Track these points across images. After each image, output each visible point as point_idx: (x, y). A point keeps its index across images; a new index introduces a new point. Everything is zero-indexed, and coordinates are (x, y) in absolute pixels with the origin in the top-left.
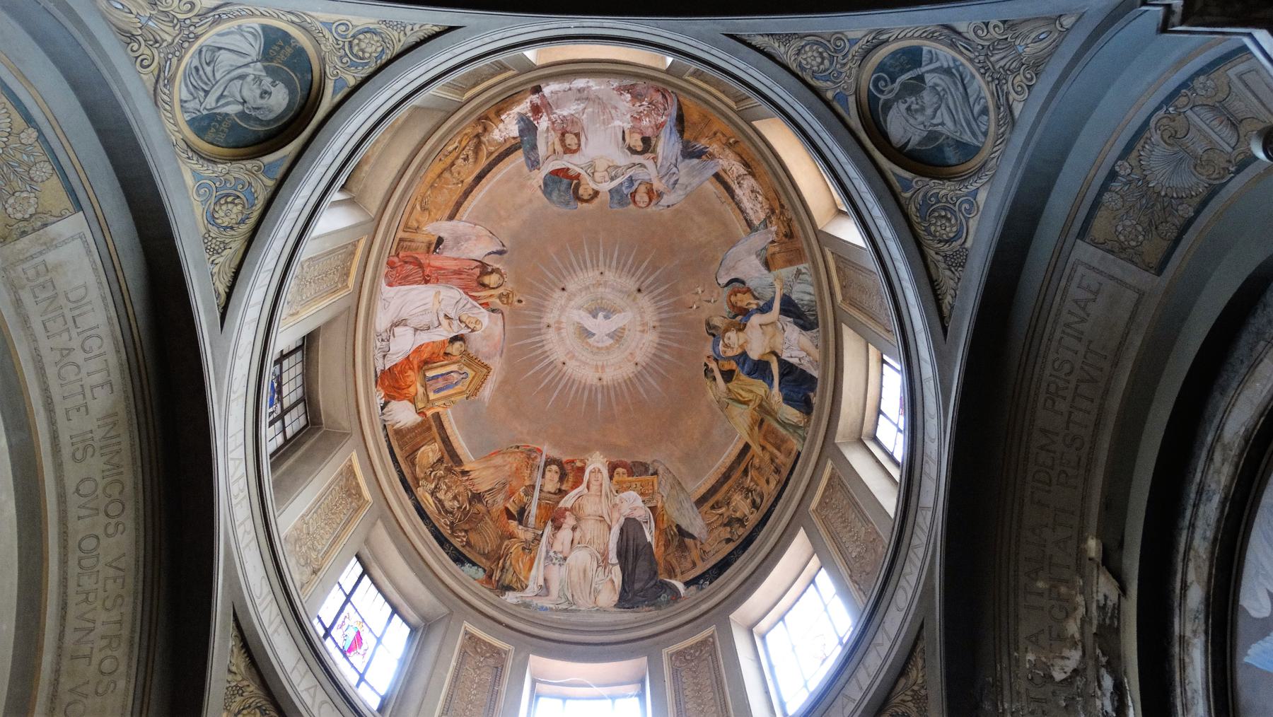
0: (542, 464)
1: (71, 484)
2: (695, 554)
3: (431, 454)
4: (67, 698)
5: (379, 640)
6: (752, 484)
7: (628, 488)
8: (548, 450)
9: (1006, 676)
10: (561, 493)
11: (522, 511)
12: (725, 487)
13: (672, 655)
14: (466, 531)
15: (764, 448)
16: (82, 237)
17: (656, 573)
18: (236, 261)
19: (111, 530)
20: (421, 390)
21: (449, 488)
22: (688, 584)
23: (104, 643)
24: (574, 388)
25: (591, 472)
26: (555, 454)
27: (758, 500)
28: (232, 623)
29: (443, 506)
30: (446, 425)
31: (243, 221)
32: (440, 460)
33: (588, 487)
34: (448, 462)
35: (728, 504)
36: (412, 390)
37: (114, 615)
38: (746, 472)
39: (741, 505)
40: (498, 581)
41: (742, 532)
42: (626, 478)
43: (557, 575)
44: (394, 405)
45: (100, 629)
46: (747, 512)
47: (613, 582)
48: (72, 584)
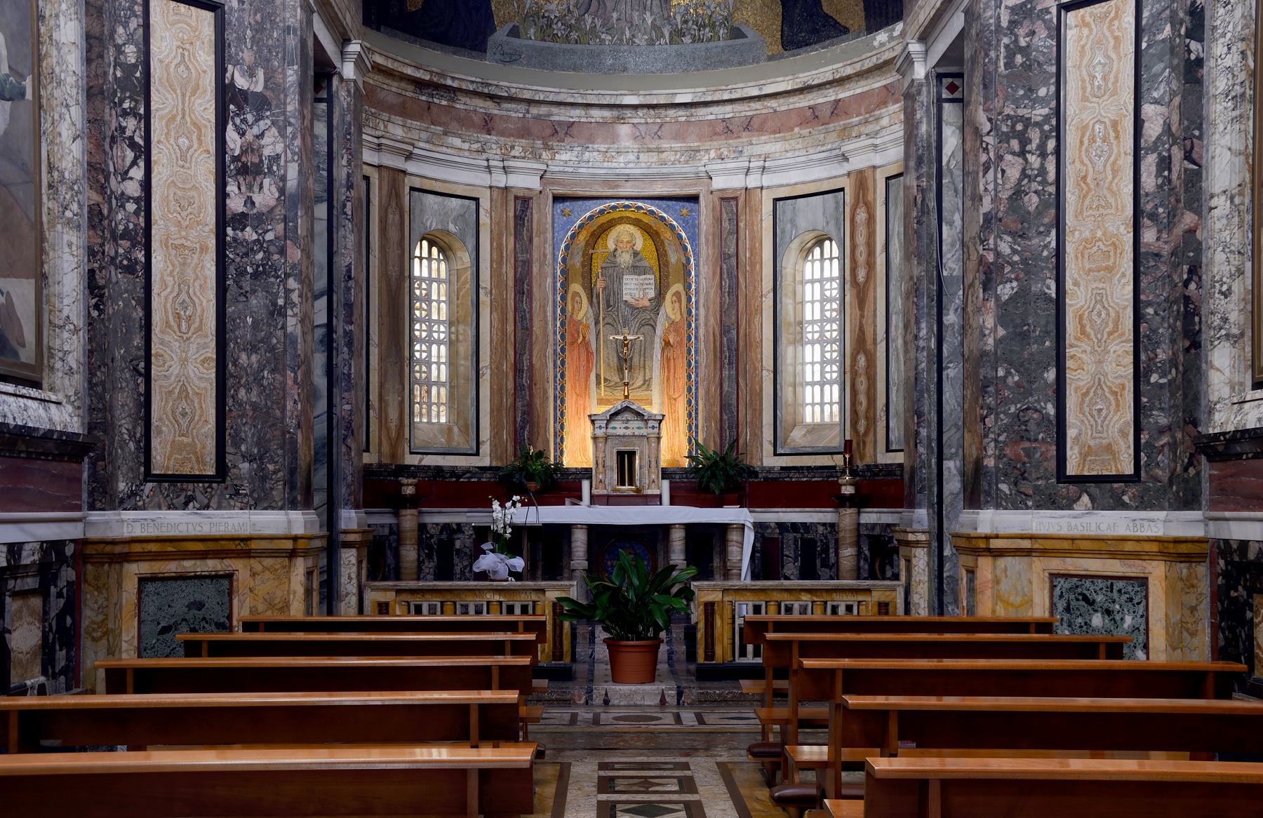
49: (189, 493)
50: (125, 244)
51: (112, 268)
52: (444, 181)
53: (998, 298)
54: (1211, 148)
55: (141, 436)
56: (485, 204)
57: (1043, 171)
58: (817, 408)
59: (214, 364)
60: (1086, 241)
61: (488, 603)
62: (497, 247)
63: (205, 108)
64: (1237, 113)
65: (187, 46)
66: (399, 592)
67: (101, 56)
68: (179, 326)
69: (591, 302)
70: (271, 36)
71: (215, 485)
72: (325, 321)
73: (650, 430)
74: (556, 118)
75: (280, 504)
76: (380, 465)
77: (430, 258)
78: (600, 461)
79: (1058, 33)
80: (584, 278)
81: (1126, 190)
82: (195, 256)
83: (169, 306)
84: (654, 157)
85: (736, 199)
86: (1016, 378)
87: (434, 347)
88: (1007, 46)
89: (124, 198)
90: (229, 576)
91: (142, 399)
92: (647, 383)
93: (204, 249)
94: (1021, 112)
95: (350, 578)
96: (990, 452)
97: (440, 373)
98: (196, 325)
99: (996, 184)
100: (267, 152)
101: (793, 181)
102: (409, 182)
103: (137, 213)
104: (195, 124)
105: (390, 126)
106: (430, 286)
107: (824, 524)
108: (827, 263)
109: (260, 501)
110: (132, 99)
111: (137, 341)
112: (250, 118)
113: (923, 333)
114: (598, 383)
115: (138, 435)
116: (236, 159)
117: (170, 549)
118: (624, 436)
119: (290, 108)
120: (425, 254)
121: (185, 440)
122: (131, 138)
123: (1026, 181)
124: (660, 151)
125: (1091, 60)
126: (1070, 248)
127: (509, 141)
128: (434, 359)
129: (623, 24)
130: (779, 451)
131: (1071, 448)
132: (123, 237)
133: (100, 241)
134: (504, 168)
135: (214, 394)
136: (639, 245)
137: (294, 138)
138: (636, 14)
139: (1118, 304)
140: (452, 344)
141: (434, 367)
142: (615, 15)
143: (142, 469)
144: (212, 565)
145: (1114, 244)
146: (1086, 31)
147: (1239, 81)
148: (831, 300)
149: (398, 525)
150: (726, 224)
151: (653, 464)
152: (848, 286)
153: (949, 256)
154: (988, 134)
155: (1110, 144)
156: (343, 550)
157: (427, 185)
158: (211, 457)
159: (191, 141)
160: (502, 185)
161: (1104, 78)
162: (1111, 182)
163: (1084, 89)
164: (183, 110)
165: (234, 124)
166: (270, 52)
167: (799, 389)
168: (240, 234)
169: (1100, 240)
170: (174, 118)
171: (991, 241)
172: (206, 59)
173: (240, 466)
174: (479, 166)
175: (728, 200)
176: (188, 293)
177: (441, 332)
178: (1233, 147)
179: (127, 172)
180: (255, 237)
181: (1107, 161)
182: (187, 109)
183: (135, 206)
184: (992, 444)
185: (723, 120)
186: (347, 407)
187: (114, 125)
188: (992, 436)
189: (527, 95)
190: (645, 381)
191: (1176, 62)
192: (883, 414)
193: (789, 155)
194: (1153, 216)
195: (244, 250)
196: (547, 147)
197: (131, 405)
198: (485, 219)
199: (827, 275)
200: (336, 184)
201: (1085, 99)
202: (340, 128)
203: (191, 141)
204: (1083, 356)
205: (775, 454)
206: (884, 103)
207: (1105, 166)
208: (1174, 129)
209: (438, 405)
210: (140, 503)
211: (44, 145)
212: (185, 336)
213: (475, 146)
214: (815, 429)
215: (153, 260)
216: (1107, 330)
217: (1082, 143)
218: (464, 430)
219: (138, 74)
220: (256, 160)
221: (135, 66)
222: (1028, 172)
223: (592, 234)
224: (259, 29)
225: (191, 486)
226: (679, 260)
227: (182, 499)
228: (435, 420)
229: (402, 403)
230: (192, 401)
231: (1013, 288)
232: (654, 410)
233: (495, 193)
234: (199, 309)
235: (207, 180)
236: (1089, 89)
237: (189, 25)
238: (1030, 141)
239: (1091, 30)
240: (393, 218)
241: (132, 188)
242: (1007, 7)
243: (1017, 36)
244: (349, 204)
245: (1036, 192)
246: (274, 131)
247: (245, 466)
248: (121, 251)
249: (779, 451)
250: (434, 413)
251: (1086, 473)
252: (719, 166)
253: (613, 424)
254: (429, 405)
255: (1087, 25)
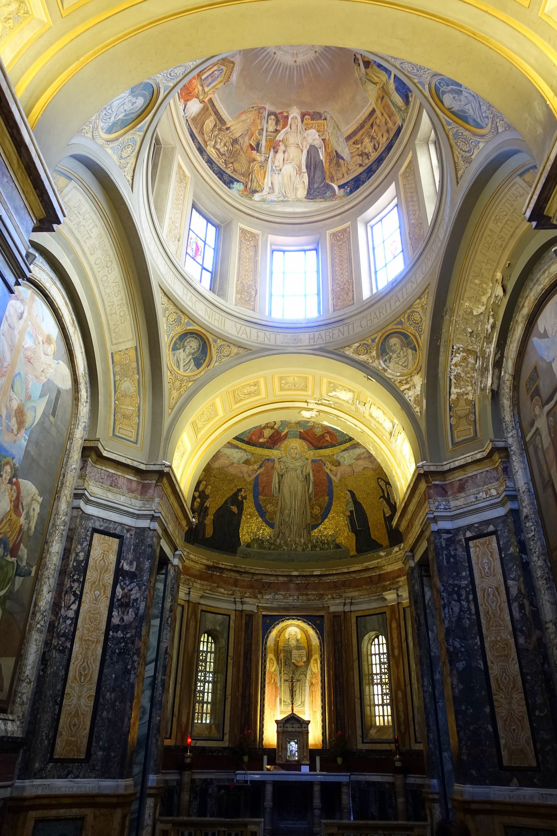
0: (266, 116)
1: (92, 262)
2: (344, 169)
3: (210, 124)
4: (113, 328)
5: (205, 242)
6: (375, 134)
7: (311, 127)
8: (269, 107)
9: (457, 308)
10: (277, 131)
11: (258, 145)
12: (361, 133)
13: (331, 234)
14: (232, 163)
15: (382, 114)
16: (75, 187)
17: (324, 178)
18: (133, 166)
19: (110, 272)
20: (200, 88)
21: (221, 140)
22: (340, 187)
23: (119, 306)
24: (281, 68)
25: (292, 118)
26: (273, 109)
27: (377, 146)
28: (159, 289)
29: (220, 152)
30: (215, 104)
31: (133, 152)
32: (215, 126)
33: (291, 128)
34: (219, 125)
35: (362, 143)
36: (196, 90)
37: (119, 297)
38: (372, 125)
39: (368, 147)
40: (250, 189)
41: (368, 162)
42: (310, 121)
43: (277, 179)
44: (189, 104)
45: (116, 303)
46: (371, 151)
47: (304, 183)
48: (103, 293)
49: (70, 769)
50: (63, 639)
51: (54, 651)
52: (216, 607)
53: (457, 669)
54: (541, 601)
55: (52, 737)
56: (233, 617)
57: (469, 609)
58: (381, 718)
59: (93, 698)
60: (493, 641)
61: (219, 832)
62: (237, 638)
63: (109, 578)
64: (549, 585)
65: (106, 553)
66: (175, 824)
67: (68, 557)
68: (80, 679)
69: (278, 664)
70: (141, 548)
71: (83, 764)
72: (152, 674)
73: (303, 729)
74: (264, 581)
75: (114, 776)
76: (175, 746)
77: (208, 642)
78: (280, 745)
79: (467, 549)
80: (275, 651)
81: (507, 618)
82: (93, 645)
83: (77, 669)
84: (305, 598)
85: (340, 616)
86: (471, 711)
87: (207, 684)
88: (446, 555)
89: (66, 618)
90: (82, 819)
91: (56, 717)
92: (303, 703)
93: (98, 642)
94: (456, 582)
95: (149, 816)
96: (464, 751)
97: (208, 697)
98: (88, 678)
99: (449, 615)
100: (133, 597)
101: (364, 609)
102: (200, 607)
103: (70, 625)
104: (103, 585)
105: (195, 584)
106: (207, 655)
107: (388, 783)
108: (381, 646)
109: (105, 774)
110: (78, 574)
111: (59, 687)
112: (127, 582)
113: (426, 683)
114: (281, 703)
115: (50, 736)
116: (119, 600)
117: (54, 802)
118: (291, 732)
119: (145, 578)
120: (206, 640)
121: (73, 739)
122: (75, 591)
123: (462, 613)
124: (307, 595)
125: (482, 561)
126: (487, 645)
127: (244, 590)
128: (206, 691)
129: (292, 543)
130: (365, 741)
131: (504, 751)
132: (62, 636)
133: (51, 638)
134: (241, 602)
135: (91, 714)
136: (299, 637)
137: (145, 591)
138: (297, 539)
139: (513, 673)
140: (214, 683)
141: (206, 694)
142: (289, 539)
143: (49, 755)
144: (75, 812)
145: (506, 644)
146: (478, 549)
147: (546, 572)
148: (384, 663)
149: (181, 780)
150: (336, 628)
151: (305, 747)
152: (390, 657)
153: (433, 646)
154: (443, 592)
155: (496, 597)
156: (148, 799)
157: (208, 609)
158: (84, 749)
159: (100, 592)
160: (240, 609)
161: (489, 569)
162: (500, 615)
163: (481, 573)
164: (100, 579)
165: (120, 585)
166: (140, 554)
167: (372, 708)
168: (115, 634)
169: (499, 642)
170: (95, 582)
171: (451, 641)
172: (113, 558)
173: (98, 753)
174: (231, 601)
175: (336, 616)
176: (87, 662)
177: (210, 677)
178: (550, 600)
179: (70, 606)
180: (122, 635)
181: (496, 605)
182: (101, 579)
183: (70, 622)
184: (464, 747)
185: (334, 582)
186: (158, 718)
187: (68, 585)
188: (464, 742)
189: (252, 571)
190: (302, 702)
191: (517, 563)
192: (412, 722)
193: (362, 597)
194: (522, 631)
195: (116, 642)
196: (260, 593)
197: (50, 720)
198: (232, 624)
199: (381, 652)
200: (165, 610)
201: (482, 577)
202: (170, 586)
203: (100, 592)
204: (501, 700)
205: (363, 742)
206: (400, 576)
207: (496, 607)
208: (523, 591)
209: (206, 714)
210: (44, 775)
211: (35, 595)
212: (82, 684)
213: (230, 592)
214: (381, 729)
215: (74, 647)
216: (511, 687)
217: (484, 597)
218: (217, 727)
219: (83, 564)
220: (127, 601)
221: (82, 561)
222: (463, 609)
223: (279, 631)
224: (136, 546)
225: (71, 765)
226: (316, 643)
227: (66, 772)
228: (204, 722)
229: (189, 713)
230: (80, 718)
231: (463, 664)
232: (305, 717)
233: (237, 613)
234: (91, 670)
235: (104, 610)
236: (483, 573)
237: (108, 544)
238: (462, 595)
239: (480, 549)
240: (192, 624)
241: (71, 614)
242: (444, 539)
243: (450, 551)
244: (170, 619)
245: (468, 618)
246: (137, 588)
247: (100, 753)
248: (60, 642)
249: (365, 741)
250: (204, 718)
251: (513, 765)
252: (332, 602)
253: (286, 725)
254: (202, 713)
255: (478, 546)
